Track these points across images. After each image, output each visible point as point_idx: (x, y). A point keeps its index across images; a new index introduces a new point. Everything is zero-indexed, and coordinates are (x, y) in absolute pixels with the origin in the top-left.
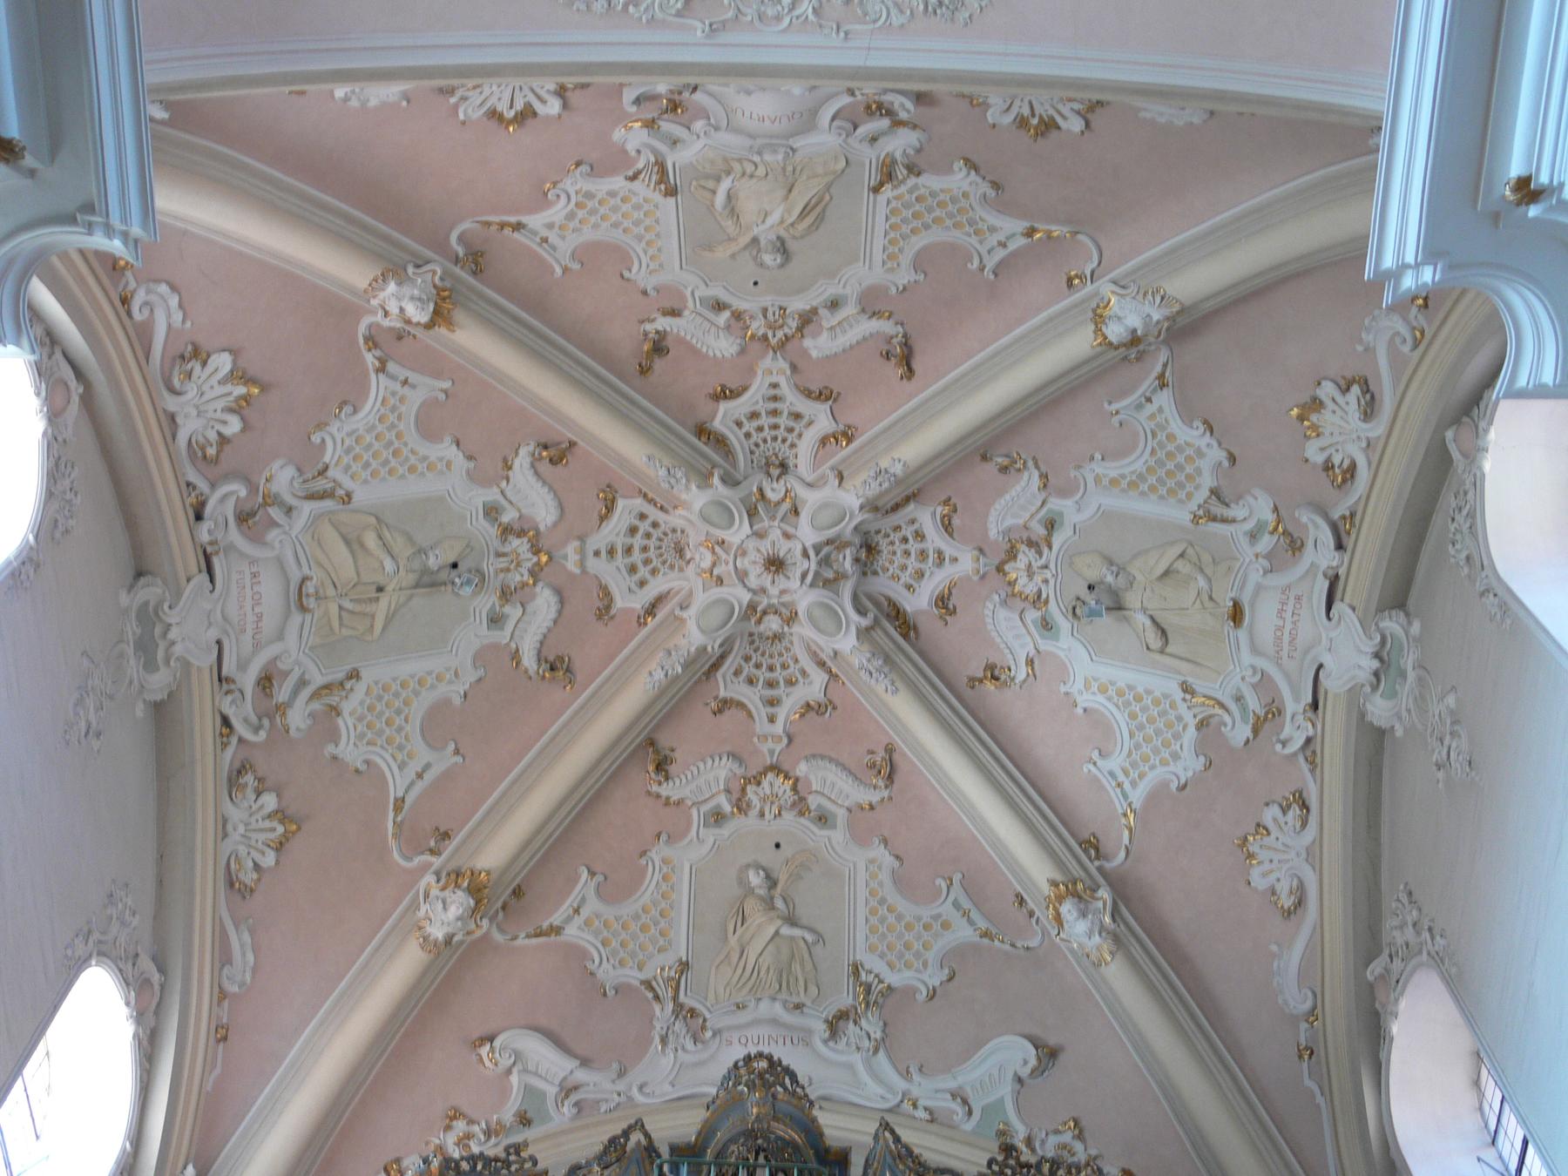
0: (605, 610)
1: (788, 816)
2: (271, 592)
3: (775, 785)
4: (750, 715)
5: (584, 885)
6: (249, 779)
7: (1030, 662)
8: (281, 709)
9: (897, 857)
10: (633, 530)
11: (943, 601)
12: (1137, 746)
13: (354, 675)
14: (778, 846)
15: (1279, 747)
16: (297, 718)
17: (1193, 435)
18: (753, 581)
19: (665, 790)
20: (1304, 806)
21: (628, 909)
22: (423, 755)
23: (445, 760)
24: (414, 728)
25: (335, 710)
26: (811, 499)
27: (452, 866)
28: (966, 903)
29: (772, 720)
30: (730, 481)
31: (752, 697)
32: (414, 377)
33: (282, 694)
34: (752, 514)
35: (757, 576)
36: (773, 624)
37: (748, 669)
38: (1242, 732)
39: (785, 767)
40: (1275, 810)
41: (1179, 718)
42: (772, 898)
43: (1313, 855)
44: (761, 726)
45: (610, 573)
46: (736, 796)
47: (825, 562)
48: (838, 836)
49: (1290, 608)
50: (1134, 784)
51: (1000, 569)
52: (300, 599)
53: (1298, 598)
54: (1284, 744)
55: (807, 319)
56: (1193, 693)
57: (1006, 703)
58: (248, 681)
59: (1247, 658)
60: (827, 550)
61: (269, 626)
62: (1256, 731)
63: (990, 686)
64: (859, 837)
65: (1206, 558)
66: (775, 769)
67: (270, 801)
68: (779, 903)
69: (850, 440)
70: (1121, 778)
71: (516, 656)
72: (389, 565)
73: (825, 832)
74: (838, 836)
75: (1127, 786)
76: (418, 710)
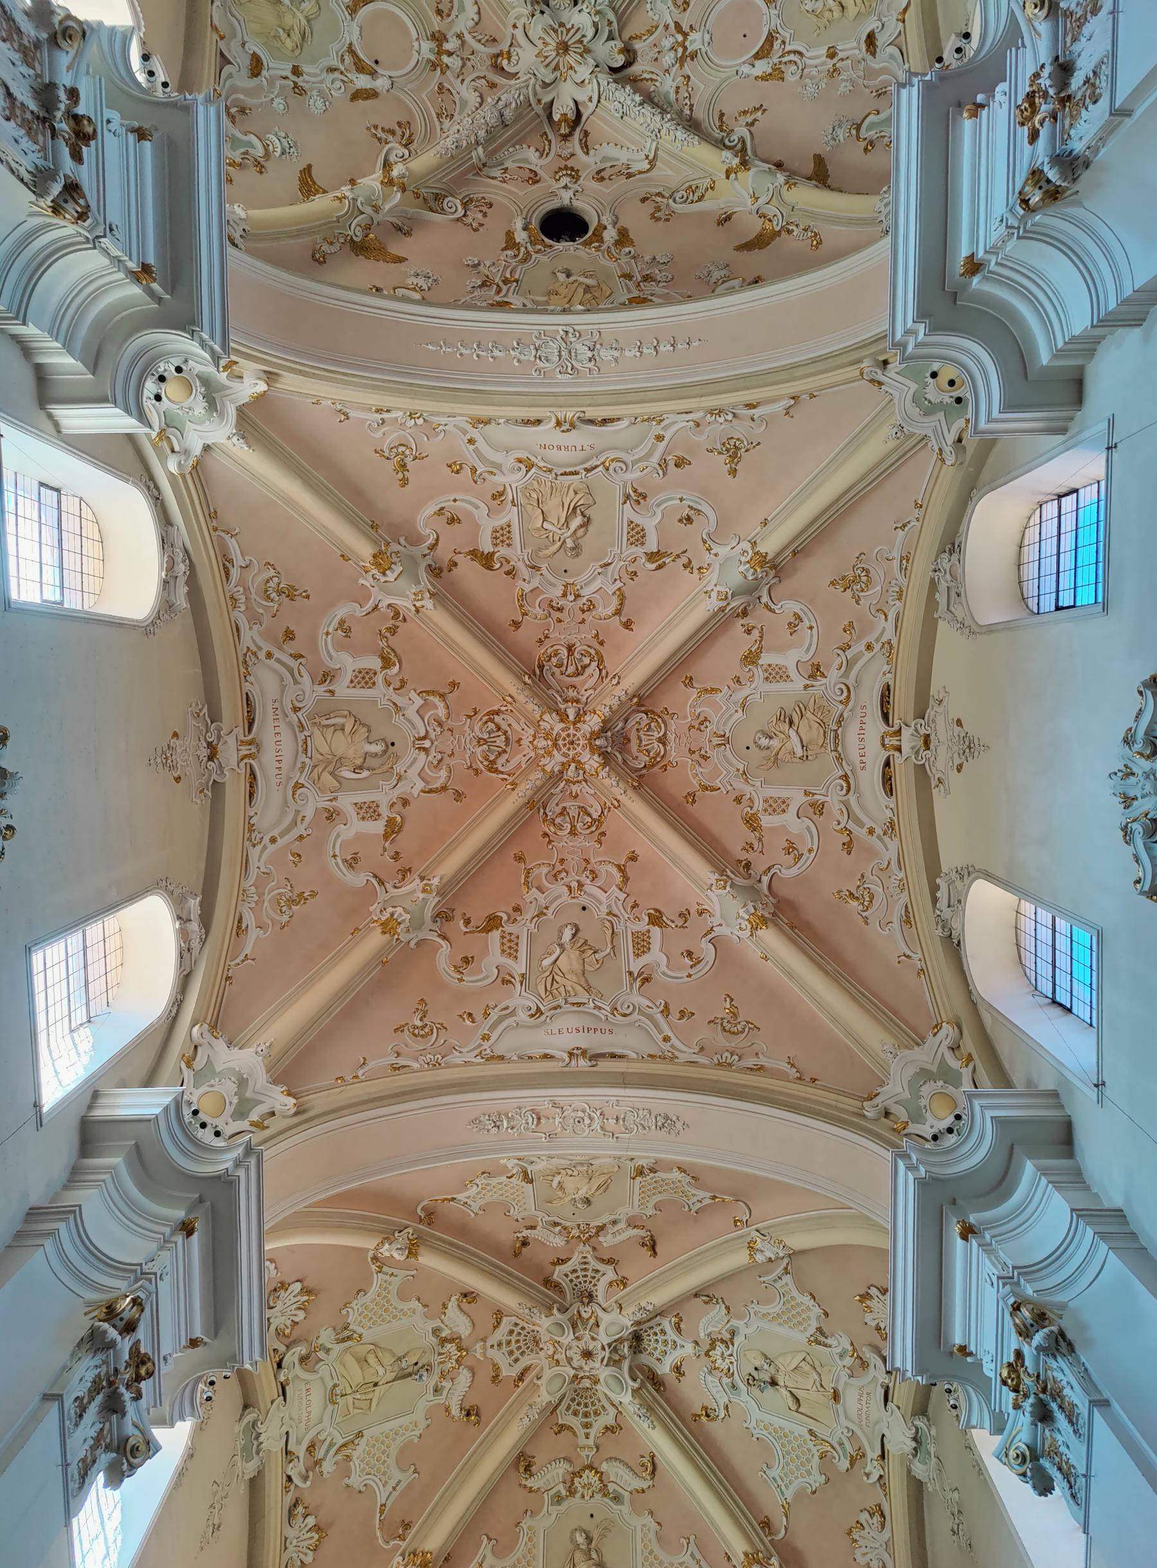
0: (495, 1378)
1: (598, 1496)
2: (317, 1398)
3: (589, 1477)
4: (574, 1434)
5: (485, 1547)
6: (300, 1509)
7: (726, 1408)
8: (318, 1463)
9: (659, 1523)
10: (511, 1332)
11: (678, 1369)
12: (787, 1464)
13: (360, 1434)
14: (592, 1516)
15: (865, 1478)
16: (327, 1467)
17: (806, 1300)
18: (575, 1363)
19: (529, 1483)
20: (883, 1515)
21: (510, 1561)
22: (397, 1475)
23: (407, 1478)
24: (391, 1461)
25: (348, 1458)
26: (605, 1319)
27: (410, 1549)
28: (698, 1556)
29: (587, 1436)
30: (563, 1310)
31: (575, 1422)
32: (395, 1272)
33: (320, 1454)
34: (574, 1326)
35: (578, 1361)
36: (586, 1383)
37: (574, 1406)
38: (845, 1464)
39: (595, 1466)
40: (866, 1515)
41: (809, 1450)
42: (590, 1550)
43: (888, 1546)
44: (582, 1441)
45: (500, 1357)
46: (568, 1484)
47: (615, 1350)
48: (625, 1508)
49: (864, 1399)
50: (787, 1487)
51: (707, 1354)
52: (332, 1397)
53: (868, 1394)
54: (868, 1475)
55: (601, 1228)
56: (815, 1436)
57: (716, 1429)
58: (301, 1451)
59: (845, 1423)
60: (614, 1347)
61: (314, 1417)
62: (852, 1463)
63: (704, 1419)
64: (636, 1510)
65: (817, 1364)
66: (591, 1467)
67: (311, 1521)
68: (594, 1555)
69: (625, 1285)
70: (780, 1482)
71: (447, 1409)
72: (381, 1371)
73: (619, 1507)
74: (625, 1508)
75: (783, 1488)
76: (394, 1450)
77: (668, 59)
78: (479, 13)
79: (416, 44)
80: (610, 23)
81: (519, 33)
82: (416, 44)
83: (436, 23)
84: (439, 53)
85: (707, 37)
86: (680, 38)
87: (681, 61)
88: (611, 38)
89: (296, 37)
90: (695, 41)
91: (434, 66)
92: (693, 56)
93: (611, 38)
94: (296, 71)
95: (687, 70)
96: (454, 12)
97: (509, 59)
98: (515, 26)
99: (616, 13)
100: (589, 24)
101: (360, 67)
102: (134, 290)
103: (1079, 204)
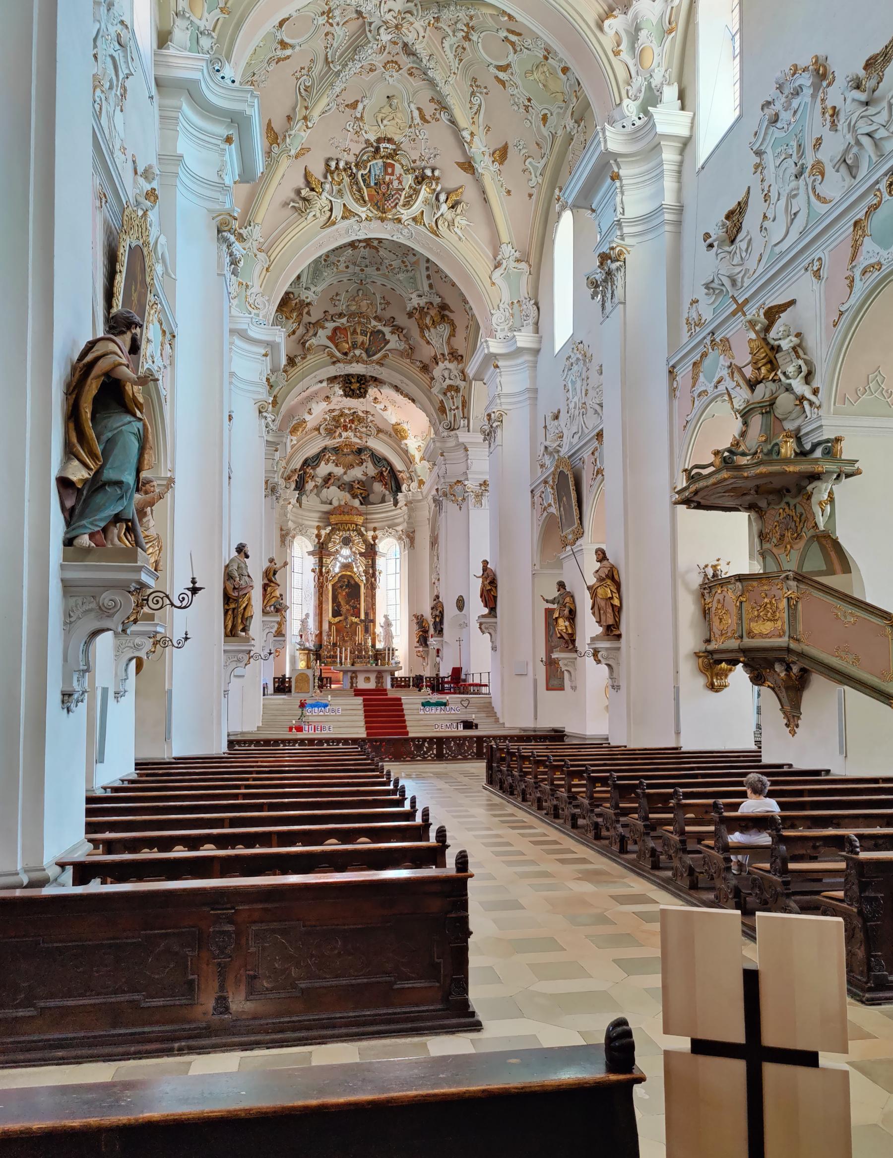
77: (337, 13)
78: (442, 43)
79: (480, 40)
80: (370, 31)
81: (422, 34)
82: (480, 40)
83: (466, 44)
84: (467, 33)
85: (315, 22)
86: (330, 21)
87: (330, 10)
88: (370, 24)
89: (541, 69)
90: (322, 20)
91: (473, 28)
92: (323, 13)
93: (370, 24)
94: (546, 58)
95: (327, 8)
96: (456, 46)
97: (429, 23)
98: (424, 37)
99: (366, 36)
100: (382, 35)
101: (513, 44)
102: (622, 172)
103: (208, 210)
